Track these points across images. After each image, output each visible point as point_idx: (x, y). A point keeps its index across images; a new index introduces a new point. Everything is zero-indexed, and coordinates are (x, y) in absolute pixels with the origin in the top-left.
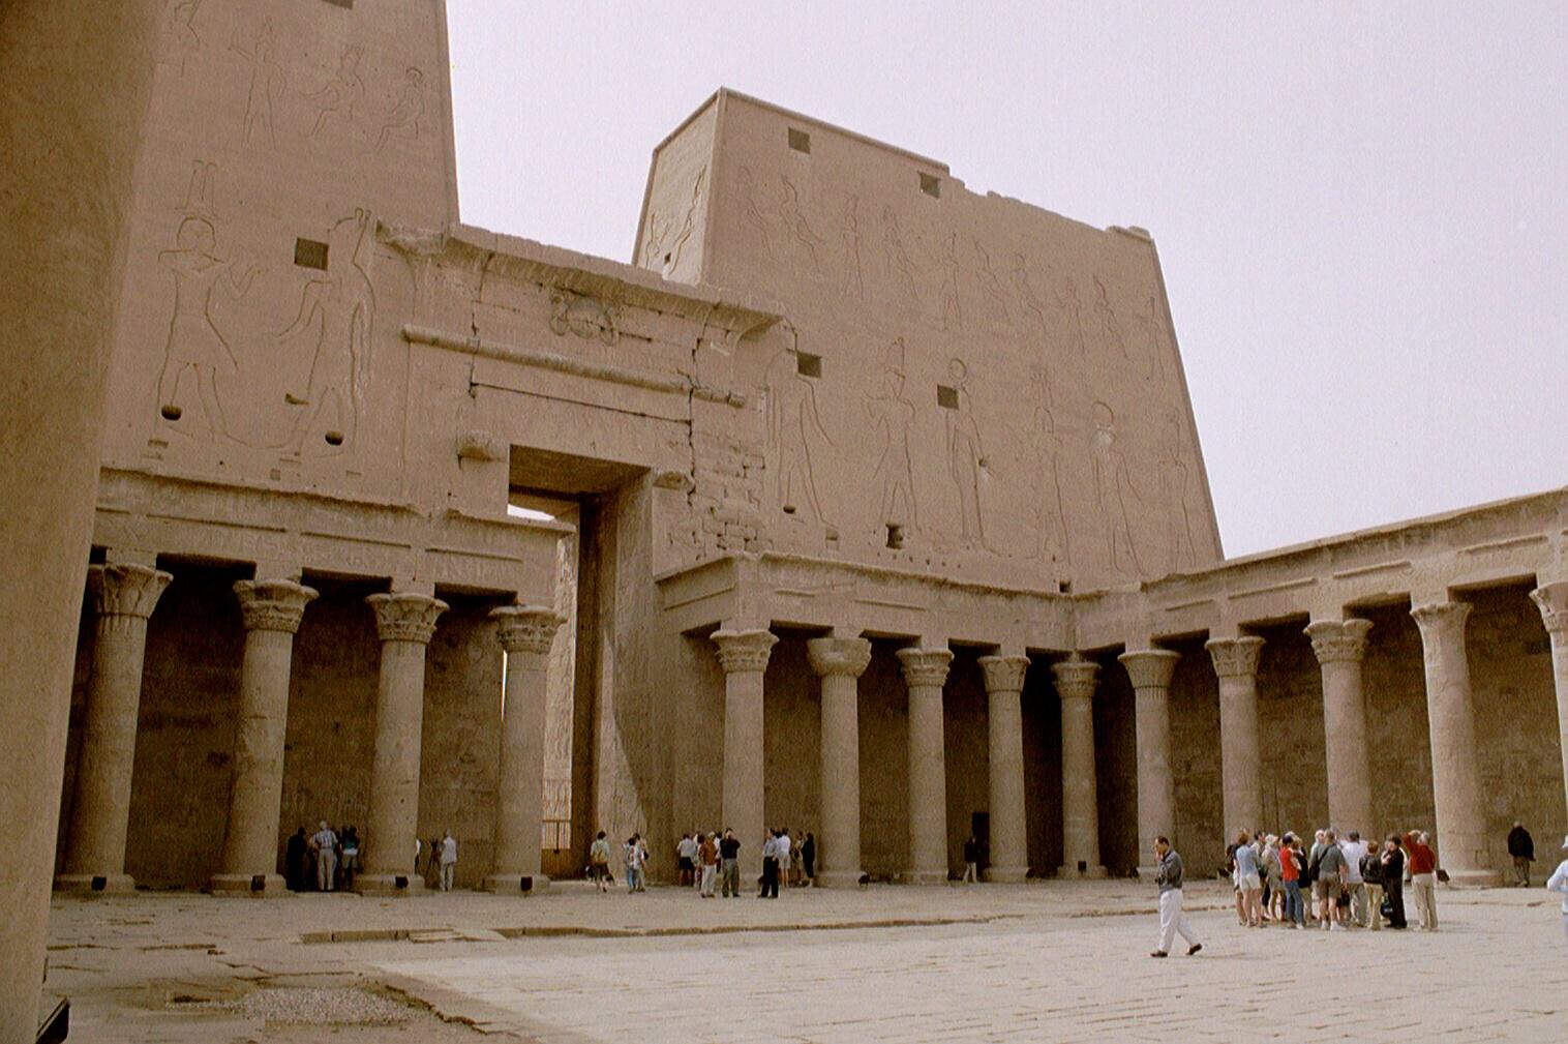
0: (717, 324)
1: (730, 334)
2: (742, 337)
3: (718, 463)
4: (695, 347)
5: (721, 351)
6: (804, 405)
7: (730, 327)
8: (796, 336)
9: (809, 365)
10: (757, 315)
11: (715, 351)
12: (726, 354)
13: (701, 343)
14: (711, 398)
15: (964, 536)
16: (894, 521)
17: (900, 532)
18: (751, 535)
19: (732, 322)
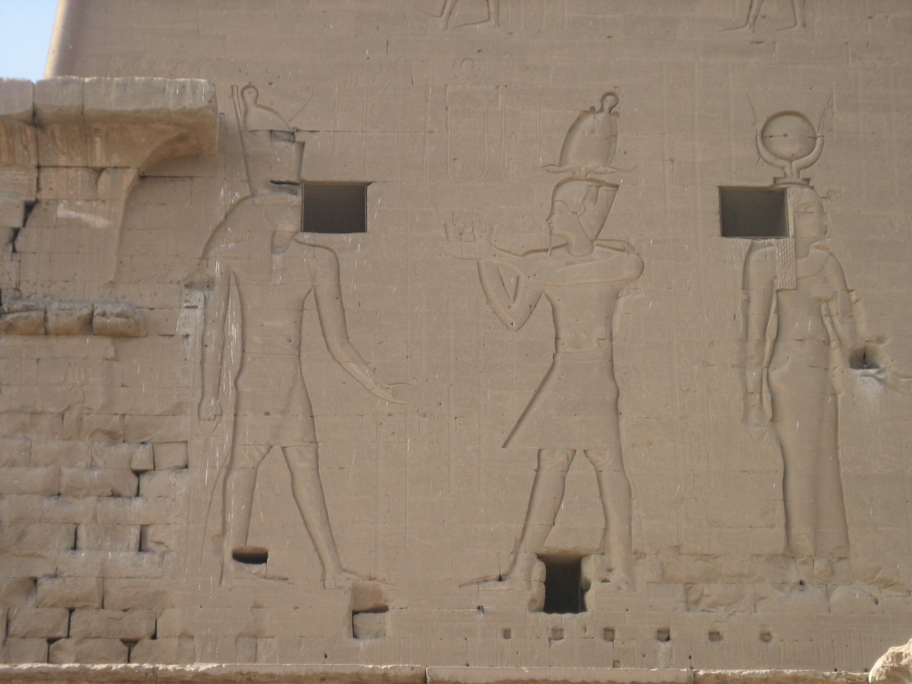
0: (63, 161)
1: (104, 178)
2: (142, 177)
3: (60, 474)
4: (18, 223)
5: (85, 217)
6: (310, 303)
7: (99, 162)
8: (302, 145)
9: (336, 209)
10: (141, 120)
11: (70, 223)
12: (100, 222)
13: (35, 211)
14: (43, 330)
15: (790, 553)
16: (560, 542)
17: (589, 570)
18: (142, 628)
19: (98, 142)
